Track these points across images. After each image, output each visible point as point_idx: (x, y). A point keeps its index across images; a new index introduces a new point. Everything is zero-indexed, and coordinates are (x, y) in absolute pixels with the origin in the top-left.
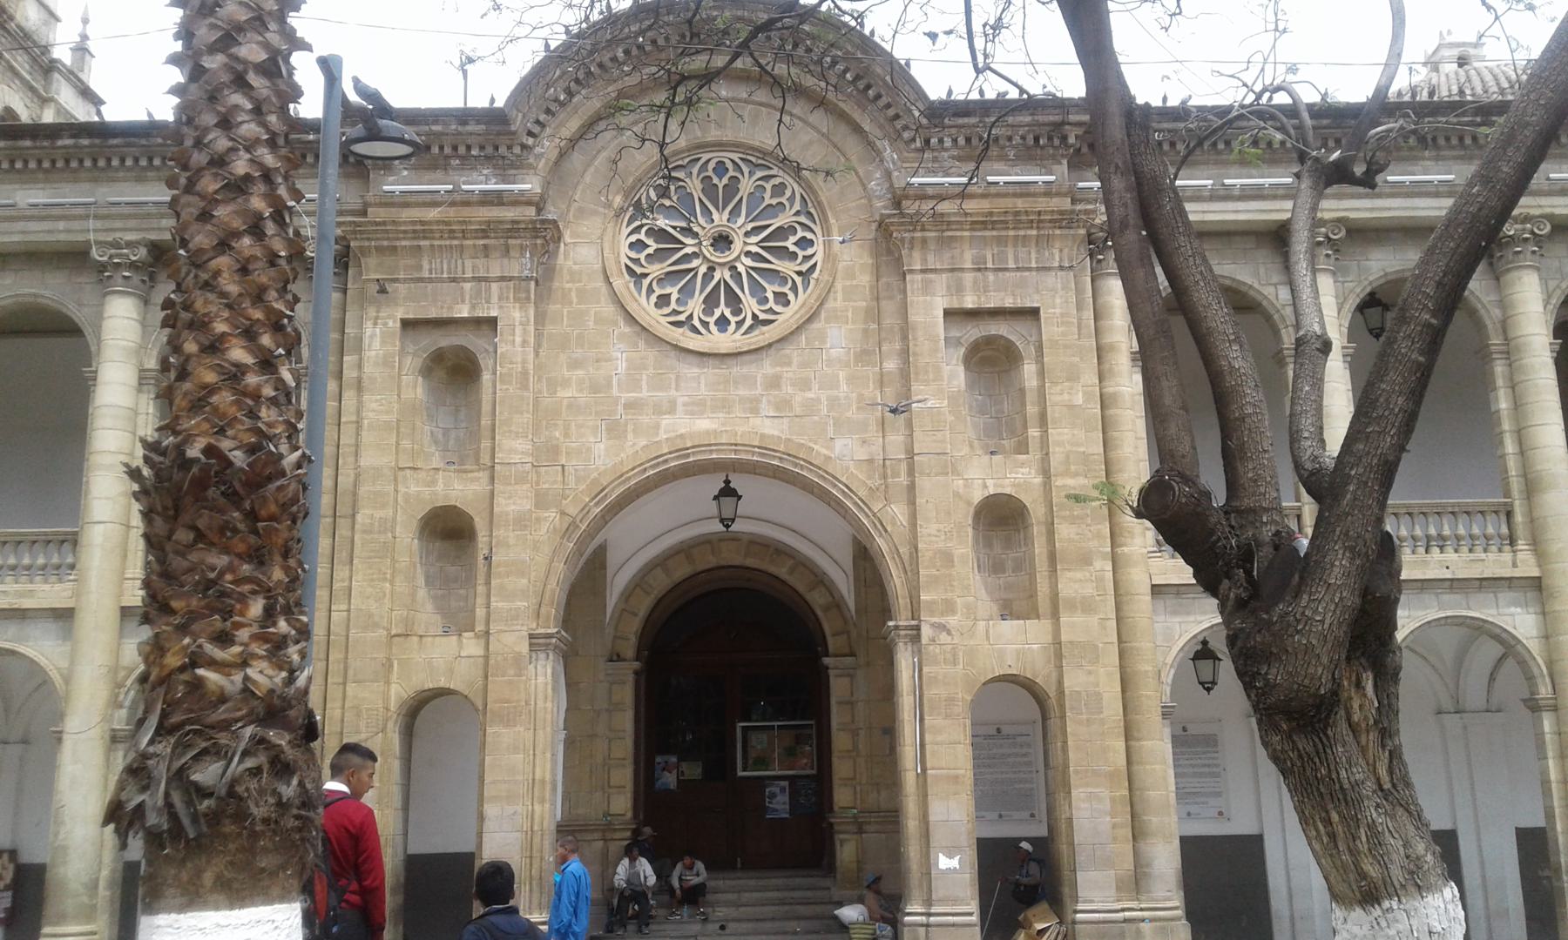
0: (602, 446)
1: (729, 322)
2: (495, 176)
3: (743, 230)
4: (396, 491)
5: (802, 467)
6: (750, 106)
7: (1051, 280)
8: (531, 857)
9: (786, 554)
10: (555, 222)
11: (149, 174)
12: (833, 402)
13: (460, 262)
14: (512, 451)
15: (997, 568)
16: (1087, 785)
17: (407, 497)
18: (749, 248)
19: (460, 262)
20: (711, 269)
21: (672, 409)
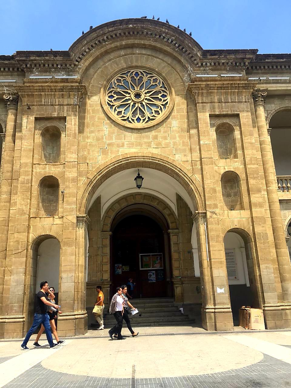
0: (100, 157)
1: (141, 120)
3: (144, 92)
4: (32, 171)
5: (165, 163)
7: (242, 106)
9: (157, 199)
10: (85, 86)
13: (54, 99)
14: (70, 158)
16: (265, 264)
17: (36, 172)
19: (54, 99)
20: (135, 104)
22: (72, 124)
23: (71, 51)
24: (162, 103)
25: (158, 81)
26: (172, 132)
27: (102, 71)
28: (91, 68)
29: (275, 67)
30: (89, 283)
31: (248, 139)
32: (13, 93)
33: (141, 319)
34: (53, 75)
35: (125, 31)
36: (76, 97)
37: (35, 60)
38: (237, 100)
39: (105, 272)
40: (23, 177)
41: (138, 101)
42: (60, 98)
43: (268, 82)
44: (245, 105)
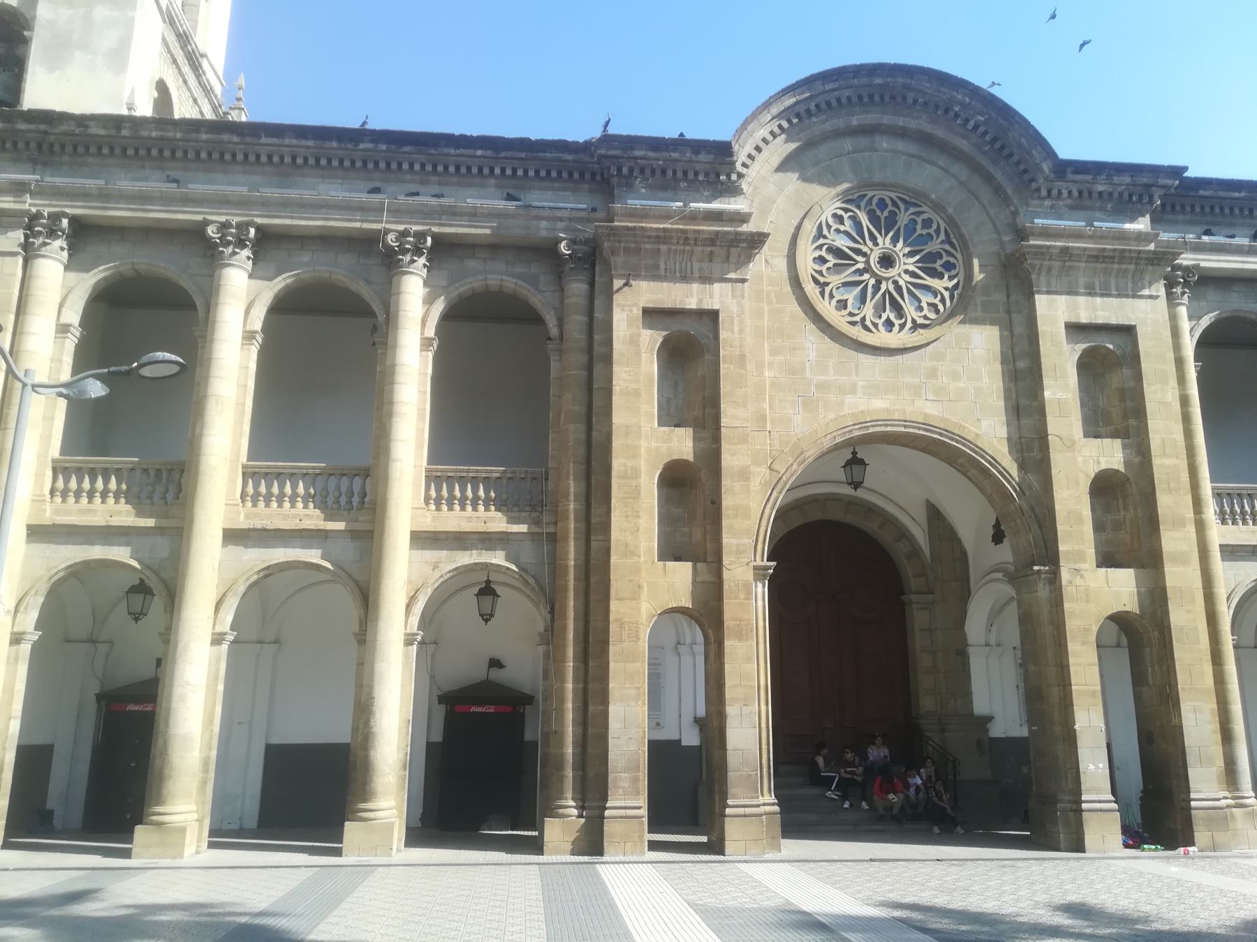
0: (799, 417)
5: (957, 441)
6: (904, 157)
11: (432, 178)
13: (689, 264)
18: (907, 267)
19: (689, 264)
20: (879, 282)
21: (853, 391)
22: (733, 331)
23: (737, 141)
25: (935, 226)
29: (1217, 210)
32: (583, 240)
37: (642, 158)
38: (1130, 289)
40: (622, 461)
42: (703, 261)
43: (1199, 248)
44: (1149, 306)
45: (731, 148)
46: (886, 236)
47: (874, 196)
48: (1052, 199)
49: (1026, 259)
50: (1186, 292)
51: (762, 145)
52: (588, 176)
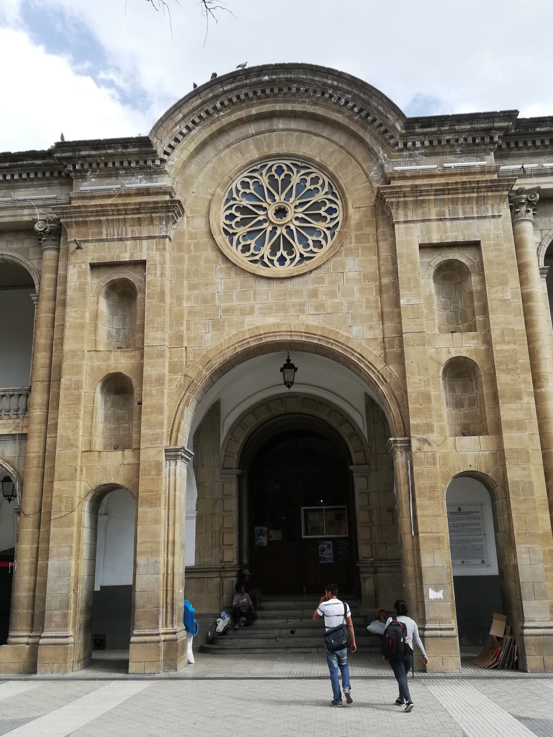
0: (209, 335)
1: (286, 260)
2: (146, 179)
3: (294, 205)
6: (296, 133)
8: (167, 590)
10: (179, 202)
12: (351, 304)
13: (124, 228)
14: (154, 338)
15: (458, 404)
19: (124, 228)
20: (275, 228)
22: (156, 273)
24: (327, 226)
25: (321, 182)
26: (346, 282)
27: (213, 168)
28: (193, 162)
30: (197, 567)
31: (497, 293)
33: (293, 640)
34: (123, 181)
35: (256, 89)
36: (164, 223)
39: (228, 547)
40: (68, 377)
41: (281, 223)
44: (492, 224)
45: (150, 141)
46: (282, 192)
47: (273, 165)
48: (409, 149)
49: (385, 199)
50: (529, 211)
51: (180, 137)
52: (56, 174)
